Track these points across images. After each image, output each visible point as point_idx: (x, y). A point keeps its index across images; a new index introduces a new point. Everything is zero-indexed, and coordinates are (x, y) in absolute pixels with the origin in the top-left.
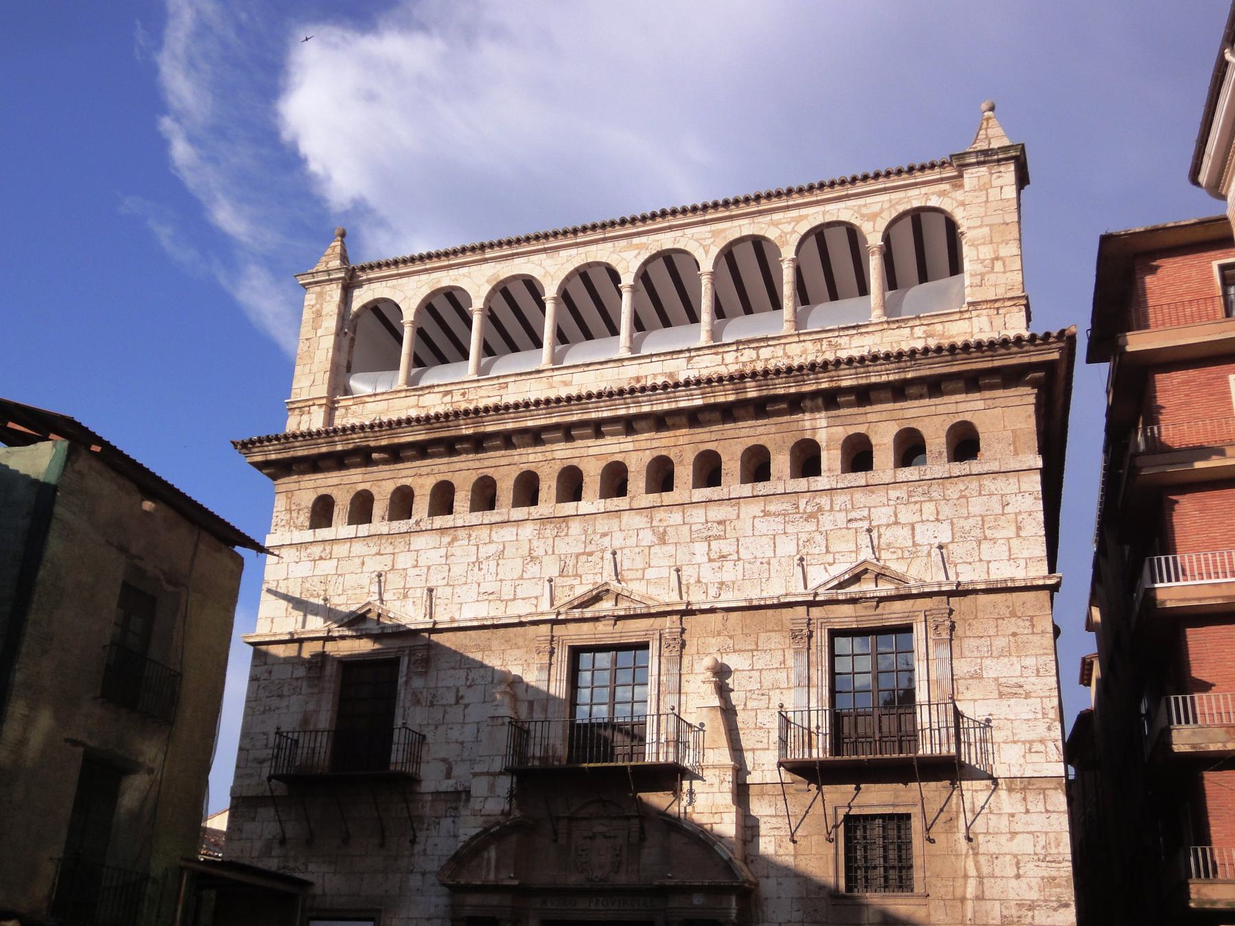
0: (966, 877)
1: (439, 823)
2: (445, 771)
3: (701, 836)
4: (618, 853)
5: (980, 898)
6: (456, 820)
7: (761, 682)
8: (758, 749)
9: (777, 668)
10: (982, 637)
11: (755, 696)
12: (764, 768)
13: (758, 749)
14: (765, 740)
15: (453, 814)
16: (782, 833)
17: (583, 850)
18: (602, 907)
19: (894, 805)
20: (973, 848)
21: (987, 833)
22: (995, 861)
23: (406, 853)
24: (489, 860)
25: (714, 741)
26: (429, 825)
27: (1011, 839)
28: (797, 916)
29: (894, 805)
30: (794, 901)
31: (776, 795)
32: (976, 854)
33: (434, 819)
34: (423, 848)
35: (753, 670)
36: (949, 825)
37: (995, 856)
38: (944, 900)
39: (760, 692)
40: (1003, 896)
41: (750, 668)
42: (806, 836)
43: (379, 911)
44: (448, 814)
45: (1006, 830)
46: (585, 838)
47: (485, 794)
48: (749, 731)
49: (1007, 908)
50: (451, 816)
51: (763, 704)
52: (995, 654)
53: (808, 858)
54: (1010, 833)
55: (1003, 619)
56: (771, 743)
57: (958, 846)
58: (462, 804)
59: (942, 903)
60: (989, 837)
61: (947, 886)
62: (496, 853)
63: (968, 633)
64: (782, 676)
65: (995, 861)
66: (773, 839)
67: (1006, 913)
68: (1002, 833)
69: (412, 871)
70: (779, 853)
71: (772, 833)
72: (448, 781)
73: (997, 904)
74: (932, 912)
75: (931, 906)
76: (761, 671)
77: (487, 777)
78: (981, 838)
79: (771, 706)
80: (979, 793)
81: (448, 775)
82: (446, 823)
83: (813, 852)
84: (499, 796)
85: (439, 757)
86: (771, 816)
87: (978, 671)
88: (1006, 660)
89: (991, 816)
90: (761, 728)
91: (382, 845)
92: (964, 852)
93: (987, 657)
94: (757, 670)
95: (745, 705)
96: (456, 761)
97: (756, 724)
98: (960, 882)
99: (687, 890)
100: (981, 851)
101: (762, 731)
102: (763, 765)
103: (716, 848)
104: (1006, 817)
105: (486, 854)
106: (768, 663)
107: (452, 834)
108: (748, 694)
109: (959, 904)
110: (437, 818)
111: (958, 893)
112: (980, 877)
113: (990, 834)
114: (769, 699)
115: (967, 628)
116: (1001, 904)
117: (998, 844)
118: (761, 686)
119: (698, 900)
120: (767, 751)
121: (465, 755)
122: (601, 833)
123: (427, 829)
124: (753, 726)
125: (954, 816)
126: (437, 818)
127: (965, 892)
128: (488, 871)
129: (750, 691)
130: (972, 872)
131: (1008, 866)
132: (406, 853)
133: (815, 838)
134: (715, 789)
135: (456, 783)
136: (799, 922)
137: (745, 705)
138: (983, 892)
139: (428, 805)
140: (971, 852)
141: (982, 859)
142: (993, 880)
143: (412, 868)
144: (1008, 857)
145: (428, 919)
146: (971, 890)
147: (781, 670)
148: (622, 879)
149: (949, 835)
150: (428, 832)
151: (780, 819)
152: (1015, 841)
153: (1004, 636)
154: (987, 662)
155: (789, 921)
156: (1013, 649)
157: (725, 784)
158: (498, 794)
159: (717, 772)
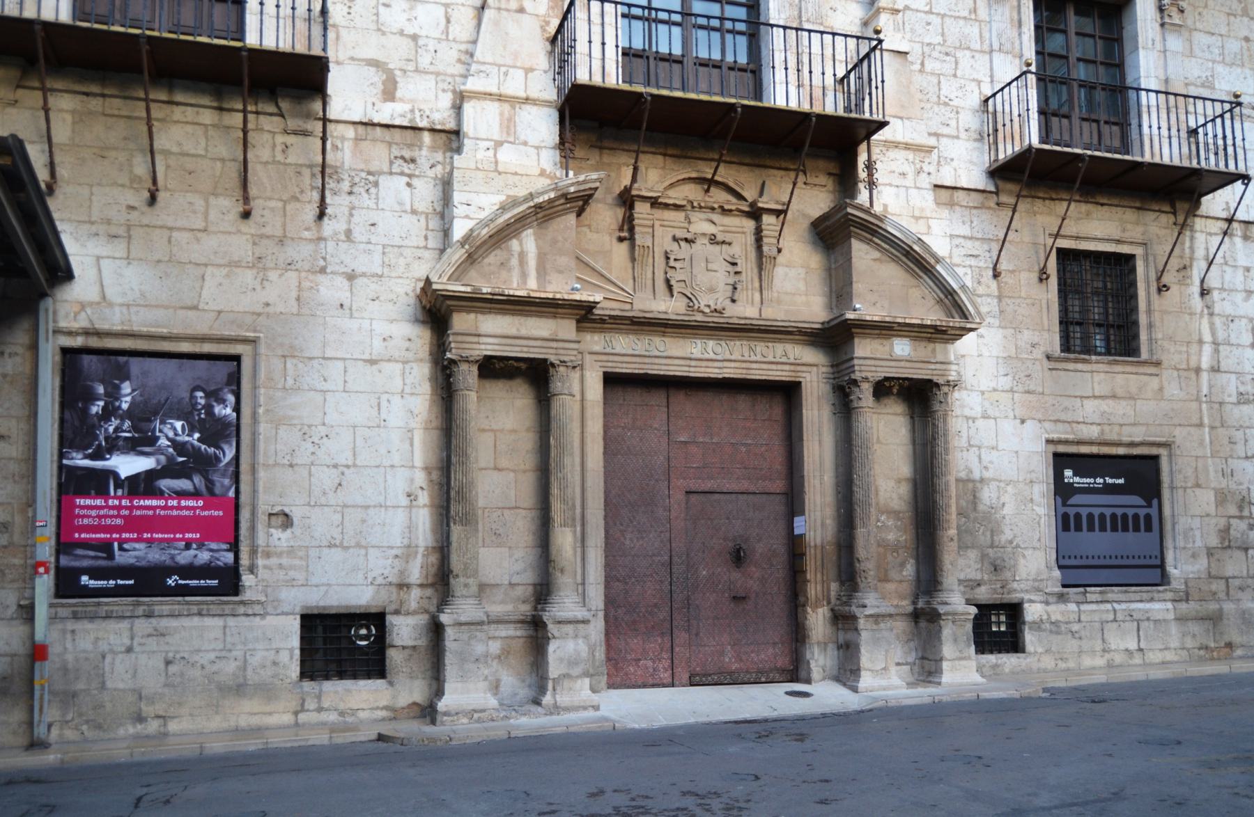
0: (1201, 342)
1: (376, 184)
2: (382, 87)
3: (916, 248)
4: (738, 269)
5: (1215, 369)
6: (415, 182)
7: (943, 35)
8: (943, 136)
9: (965, 18)
10: (1213, 34)
11: (935, 54)
12: (955, 164)
13: (943, 136)
14: (953, 123)
15: (407, 171)
16: (982, 264)
17: (675, 260)
18: (712, 356)
19: (1119, 242)
20: (1208, 307)
21: (1222, 289)
22: (1231, 325)
23: (307, 234)
24: (522, 256)
25: (903, 106)
26: (353, 185)
27: (1246, 299)
28: (1005, 382)
29: (1119, 242)
30: (1000, 361)
31: (971, 208)
32: (1211, 314)
33: (364, 175)
34: (343, 227)
35: (930, 12)
36: (1182, 273)
37: (1230, 319)
38: (1178, 370)
39: (944, 49)
40: (1239, 369)
41: (927, 8)
42: (1012, 272)
43: (253, 342)
44: (395, 169)
45: (1240, 287)
46: (675, 239)
47: (497, 137)
48: (929, 106)
49: (1243, 383)
50: (402, 174)
51: (948, 68)
52: (1227, 59)
53: (1018, 301)
54: (1246, 291)
55: (1235, 16)
56: (962, 130)
57: (1193, 302)
58: (424, 152)
59: (1175, 373)
60: (1224, 295)
61: (1180, 352)
62: (538, 247)
63: (1199, 25)
64: (973, 31)
65: (1231, 325)
66: (969, 271)
67: (1242, 389)
68: (1237, 290)
69: (323, 270)
70: (978, 292)
71: (968, 263)
72: (390, 105)
73: (1233, 377)
74: (1165, 384)
75: (1164, 377)
76: (943, 16)
77: (496, 104)
78: (1215, 294)
79: (959, 73)
80: (1214, 237)
81: (389, 94)
82: (393, 187)
83: (1023, 294)
84: (525, 143)
85: (369, 57)
86: (964, 237)
87: (1210, 79)
88: (1239, 70)
89: (1226, 268)
90: (946, 104)
91: (246, 215)
92: (1199, 311)
93: (1219, 62)
94: (938, 14)
95: (922, 64)
96: (405, 71)
97: (939, 97)
98: (1194, 348)
99: (885, 329)
100: (1217, 310)
101: (948, 108)
102: (952, 160)
103: (939, 268)
104: (1240, 272)
105: (514, 244)
106: (953, 6)
107: (408, 208)
108: (926, 49)
109: (1193, 376)
110: (369, 173)
111: (1193, 364)
112: (1215, 343)
113: (1225, 290)
114: (957, 63)
115: (1197, 17)
116: (1237, 379)
117: (1234, 304)
118: (945, 41)
119: (902, 347)
120: (956, 140)
121: (424, 61)
122: (704, 234)
123: (350, 193)
124: (935, 99)
125: (1188, 264)
126: (369, 173)
127: (1199, 361)
128: (524, 276)
129: (929, 44)
130: (1207, 337)
131: (1244, 331)
132: (307, 234)
133: (1024, 276)
134: (909, 181)
135: (412, 111)
136: (1007, 391)
137: (922, 64)
138: (1219, 362)
139: (348, 147)
140: (1206, 311)
141: (1217, 321)
142: (1228, 348)
143: (322, 263)
144: (1244, 321)
145: (372, 362)
146: (1206, 362)
147: (971, 22)
148: (746, 310)
149: (1183, 287)
150: (352, 198)
151: (977, 243)
152: (1251, 301)
153: (1236, 38)
154: (1219, 68)
155: (995, 390)
156: (1245, 57)
157: (924, 175)
158: (522, 138)
159: (910, 155)
